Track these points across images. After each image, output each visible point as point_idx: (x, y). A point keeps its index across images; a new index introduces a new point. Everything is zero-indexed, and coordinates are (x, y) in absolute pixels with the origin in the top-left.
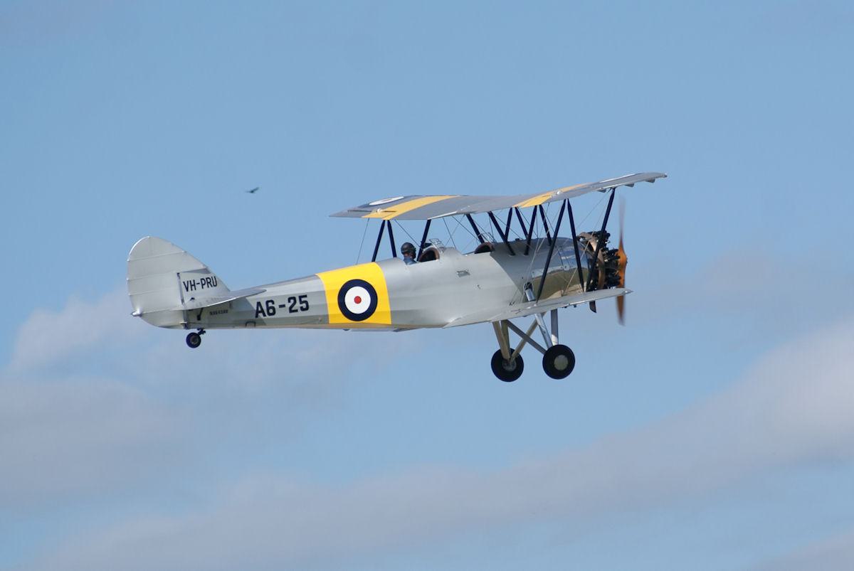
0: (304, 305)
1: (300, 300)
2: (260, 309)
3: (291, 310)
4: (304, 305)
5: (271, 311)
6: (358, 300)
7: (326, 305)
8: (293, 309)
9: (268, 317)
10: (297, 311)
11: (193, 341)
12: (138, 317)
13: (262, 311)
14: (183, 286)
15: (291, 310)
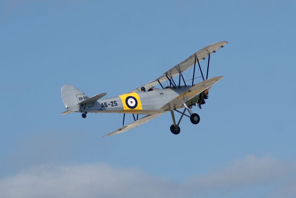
0: (116, 104)
1: (114, 102)
2: (103, 105)
3: (112, 106)
4: (116, 104)
5: (106, 106)
6: (132, 102)
7: (122, 104)
8: (113, 105)
9: (105, 108)
10: (114, 106)
11: (84, 116)
12: (67, 109)
13: (103, 106)
14: (78, 99)
15: (112, 106)
